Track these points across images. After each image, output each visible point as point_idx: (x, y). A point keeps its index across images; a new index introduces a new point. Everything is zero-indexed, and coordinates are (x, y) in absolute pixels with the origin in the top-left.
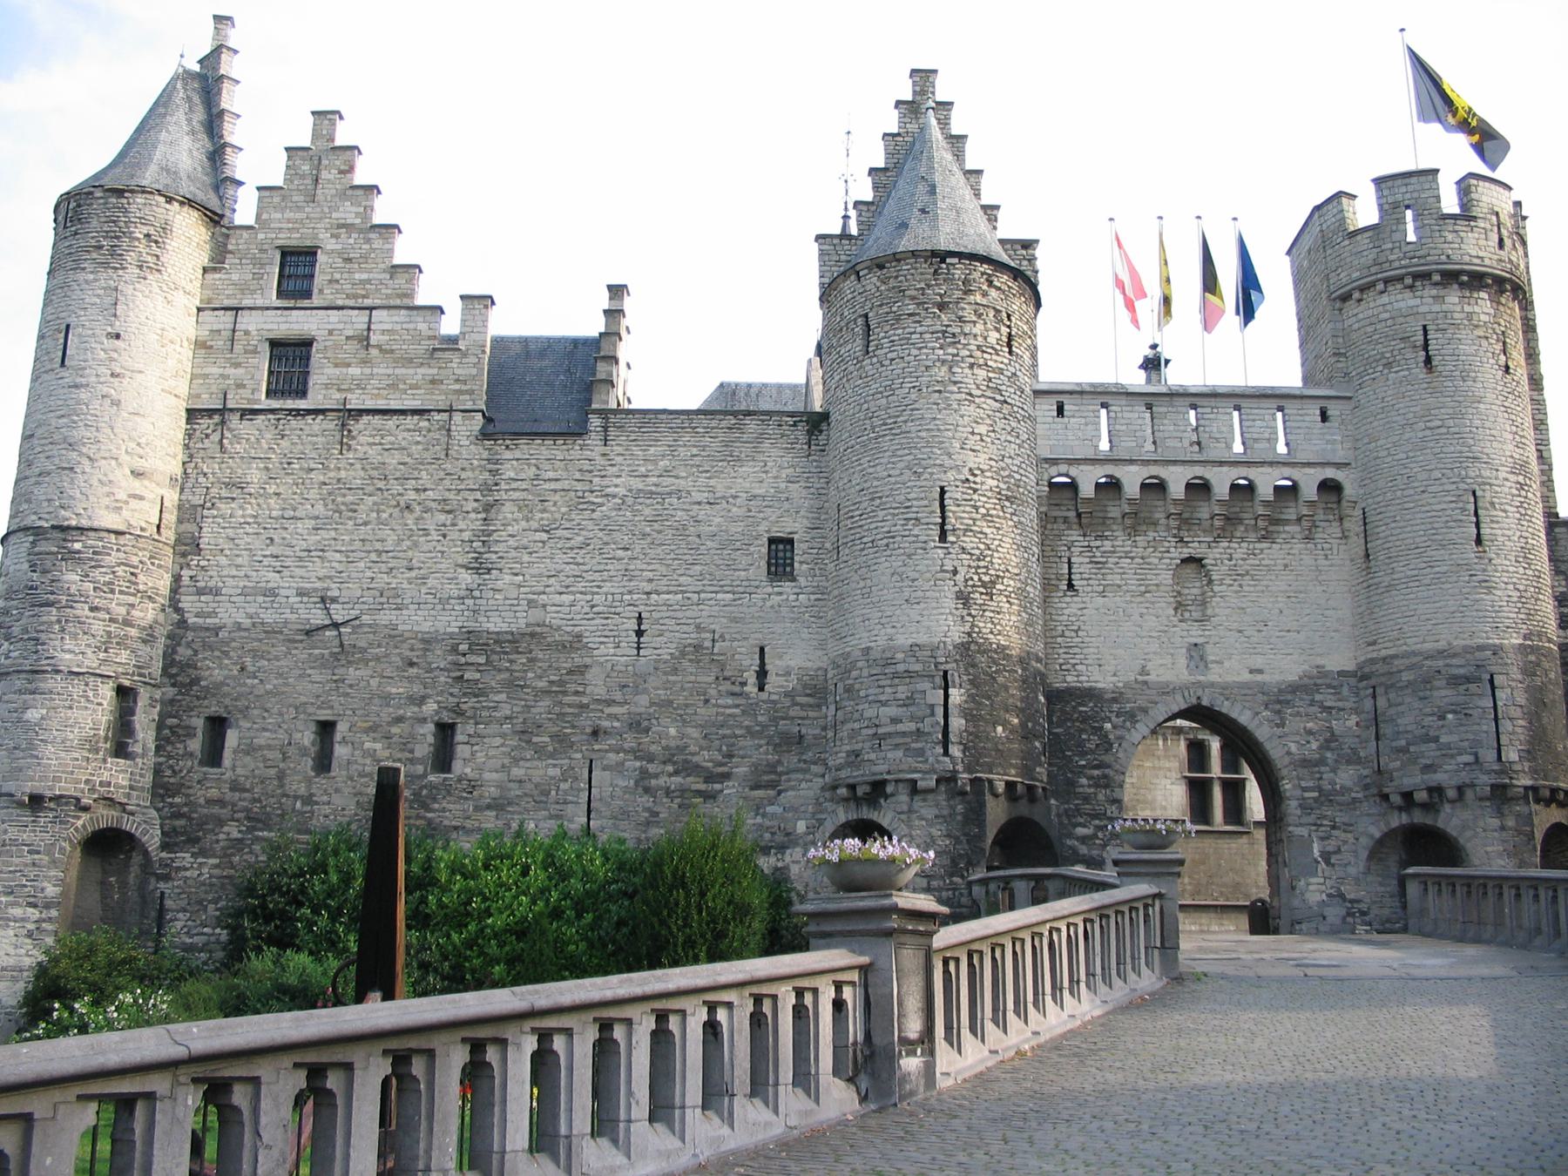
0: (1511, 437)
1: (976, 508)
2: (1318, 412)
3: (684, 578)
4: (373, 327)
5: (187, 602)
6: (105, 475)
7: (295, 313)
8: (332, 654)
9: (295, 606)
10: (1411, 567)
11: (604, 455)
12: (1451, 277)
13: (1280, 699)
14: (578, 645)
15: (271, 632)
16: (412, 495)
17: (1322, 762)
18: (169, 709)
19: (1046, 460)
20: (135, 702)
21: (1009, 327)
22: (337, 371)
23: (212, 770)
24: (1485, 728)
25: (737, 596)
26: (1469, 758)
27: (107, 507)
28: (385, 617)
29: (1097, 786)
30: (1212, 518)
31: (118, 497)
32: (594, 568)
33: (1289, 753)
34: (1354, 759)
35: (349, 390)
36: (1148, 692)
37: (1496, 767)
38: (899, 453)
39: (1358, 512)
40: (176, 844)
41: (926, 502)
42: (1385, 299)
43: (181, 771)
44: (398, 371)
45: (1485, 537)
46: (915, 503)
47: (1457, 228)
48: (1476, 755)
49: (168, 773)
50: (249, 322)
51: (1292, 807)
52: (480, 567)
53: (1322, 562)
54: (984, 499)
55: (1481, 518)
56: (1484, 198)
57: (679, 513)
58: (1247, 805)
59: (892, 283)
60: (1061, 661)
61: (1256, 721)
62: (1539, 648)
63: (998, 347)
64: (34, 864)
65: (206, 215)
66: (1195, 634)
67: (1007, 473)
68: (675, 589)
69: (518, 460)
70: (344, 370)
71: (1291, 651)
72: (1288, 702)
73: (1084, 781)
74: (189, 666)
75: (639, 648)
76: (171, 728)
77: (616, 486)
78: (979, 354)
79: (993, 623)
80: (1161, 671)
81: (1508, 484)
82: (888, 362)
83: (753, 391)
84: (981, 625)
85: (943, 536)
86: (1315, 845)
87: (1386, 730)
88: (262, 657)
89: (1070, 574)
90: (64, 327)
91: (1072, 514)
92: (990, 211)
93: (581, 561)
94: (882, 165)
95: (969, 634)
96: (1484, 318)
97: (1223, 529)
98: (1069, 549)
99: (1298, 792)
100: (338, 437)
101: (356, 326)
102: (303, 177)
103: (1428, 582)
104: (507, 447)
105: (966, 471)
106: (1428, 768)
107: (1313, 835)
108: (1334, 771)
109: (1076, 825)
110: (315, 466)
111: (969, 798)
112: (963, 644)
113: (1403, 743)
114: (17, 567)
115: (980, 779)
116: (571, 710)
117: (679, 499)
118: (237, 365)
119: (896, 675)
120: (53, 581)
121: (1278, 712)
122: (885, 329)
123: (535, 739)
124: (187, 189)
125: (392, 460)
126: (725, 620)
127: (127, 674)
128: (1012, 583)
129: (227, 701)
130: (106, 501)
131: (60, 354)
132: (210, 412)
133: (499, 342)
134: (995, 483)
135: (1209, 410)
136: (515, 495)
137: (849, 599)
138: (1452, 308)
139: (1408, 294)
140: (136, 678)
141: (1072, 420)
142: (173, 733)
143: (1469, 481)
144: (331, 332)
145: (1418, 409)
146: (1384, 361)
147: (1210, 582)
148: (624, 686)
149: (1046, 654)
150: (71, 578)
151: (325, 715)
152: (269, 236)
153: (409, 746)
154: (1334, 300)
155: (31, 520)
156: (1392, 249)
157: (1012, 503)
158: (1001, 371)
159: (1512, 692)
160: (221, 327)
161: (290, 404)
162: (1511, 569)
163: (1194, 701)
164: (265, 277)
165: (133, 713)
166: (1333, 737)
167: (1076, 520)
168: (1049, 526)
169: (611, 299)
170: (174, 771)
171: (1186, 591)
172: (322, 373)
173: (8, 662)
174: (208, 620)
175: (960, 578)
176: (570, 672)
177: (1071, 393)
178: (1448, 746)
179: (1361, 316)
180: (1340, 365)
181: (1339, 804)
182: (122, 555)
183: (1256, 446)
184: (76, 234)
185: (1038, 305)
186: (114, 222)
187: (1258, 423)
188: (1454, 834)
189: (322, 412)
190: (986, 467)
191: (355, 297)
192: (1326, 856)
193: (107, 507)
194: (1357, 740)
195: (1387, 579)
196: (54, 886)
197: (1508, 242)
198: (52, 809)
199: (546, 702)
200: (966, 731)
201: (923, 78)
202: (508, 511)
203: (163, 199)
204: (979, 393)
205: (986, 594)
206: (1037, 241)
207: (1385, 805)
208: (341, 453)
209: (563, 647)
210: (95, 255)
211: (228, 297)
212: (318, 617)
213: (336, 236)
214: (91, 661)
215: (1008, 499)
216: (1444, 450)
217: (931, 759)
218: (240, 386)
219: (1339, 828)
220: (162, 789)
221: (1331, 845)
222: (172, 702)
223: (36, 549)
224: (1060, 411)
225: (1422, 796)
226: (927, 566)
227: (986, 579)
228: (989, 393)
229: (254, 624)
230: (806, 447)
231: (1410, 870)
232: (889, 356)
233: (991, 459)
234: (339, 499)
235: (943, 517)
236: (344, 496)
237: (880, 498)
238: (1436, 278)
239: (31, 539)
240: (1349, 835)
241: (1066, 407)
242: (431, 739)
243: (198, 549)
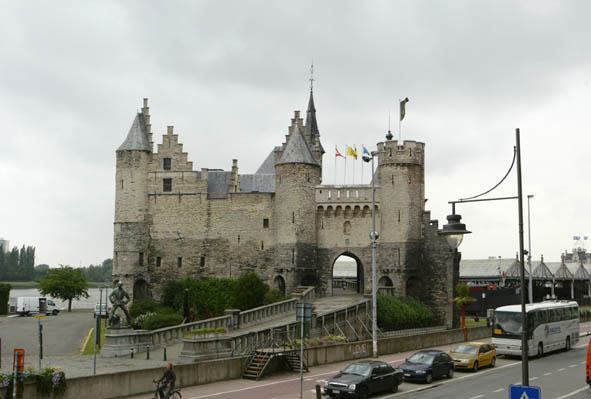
5: (152, 234)
12: (398, 164)
13: (364, 250)
15: (168, 240)
50: (159, 175)
52: (208, 226)
66: (347, 237)
112: (297, 244)
159: (403, 253)
202: (213, 215)
212: (177, 237)
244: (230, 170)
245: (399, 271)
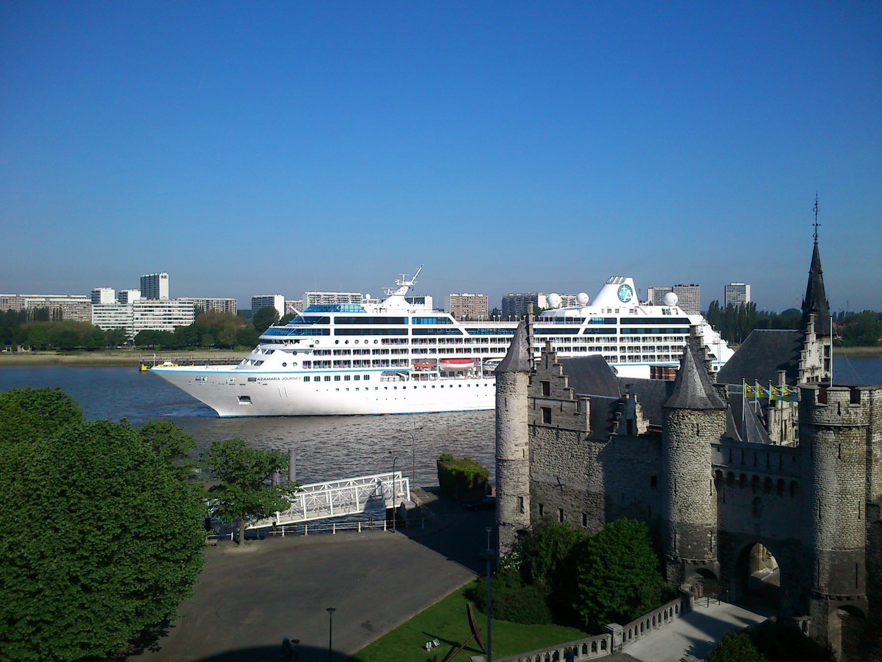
5: (533, 474)
28: (571, 484)
96: (830, 440)
130: (510, 453)
144: (554, 406)
158: (693, 443)
197: (843, 412)
214: (511, 492)
215: (695, 481)
227: (686, 505)
228: (689, 450)
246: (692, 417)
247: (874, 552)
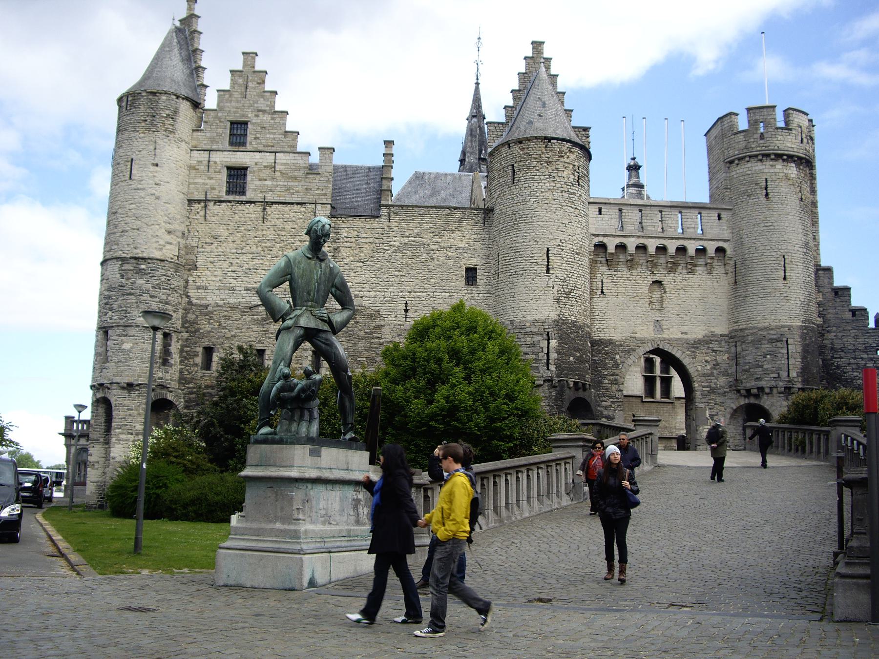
0: (802, 231)
1: (562, 258)
2: (717, 215)
3: (427, 285)
4: (277, 161)
5: (192, 293)
6: (154, 233)
7: (238, 153)
8: (262, 318)
9: (244, 295)
10: (755, 289)
11: (388, 226)
12: (779, 156)
13: (695, 346)
14: (378, 316)
15: (233, 308)
16: (298, 243)
17: (712, 374)
18: (187, 343)
19: (594, 235)
20: (171, 340)
21: (578, 173)
22: (260, 183)
23: (206, 372)
24: (783, 362)
25: (451, 294)
26: (775, 375)
27: (156, 248)
29: (612, 384)
30: (667, 263)
31: (162, 243)
32: (385, 280)
33: (697, 371)
34: (725, 374)
35: (266, 192)
36: (636, 342)
37: (787, 380)
38: (528, 231)
39: (732, 263)
40: (191, 406)
41: (541, 255)
42: (749, 165)
43: (192, 372)
44: (289, 184)
45: (787, 277)
46: (535, 255)
47: (783, 134)
48: (779, 374)
49: (186, 373)
50: (217, 157)
51: (698, 394)
53: (715, 284)
54: (567, 254)
55: (787, 268)
56: (795, 120)
57: (424, 255)
58: (672, 389)
59: (526, 151)
60: (598, 327)
61: (683, 356)
62: (808, 327)
63: (574, 183)
64: (130, 415)
65: (193, 104)
66: (657, 316)
67: (576, 242)
68: (422, 290)
69: (348, 228)
70: (264, 182)
71: (700, 324)
72: (697, 348)
73: (606, 381)
74: (194, 323)
75: (406, 318)
76: (186, 352)
77: (395, 241)
78: (565, 186)
79: (569, 310)
80: (642, 332)
81: (799, 253)
82: (524, 189)
83: (432, 176)
84: (564, 311)
85: (548, 271)
86: (707, 411)
87: (741, 361)
88: (229, 319)
89: (602, 287)
90: (130, 159)
91: (603, 260)
92: (569, 112)
93: (379, 276)
94: (517, 88)
95: (559, 316)
96: (793, 176)
97: (671, 268)
98: (602, 275)
99: (701, 388)
100: (262, 214)
101: (268, 161)
102: (239, 85)
103: (762, 296)
104: (343, 221)
105: (559, 240)
106: (758, 379)
107: (707, 407)
108: (717, 379)
109: (602, 401)
110: (251, 229)
111: (558, 389)
113: (747, 367)
114: (113, 276)
115: (563, 380)
116: (375, 346)
117: (424, 248)
118: (211, 178)
119: (526, 333)
120: (132, 283)
121: (694, 352)
122: (522, 173)
123: (359, 359)
124: (184, 92)
125: (288, 227)
126: (445, 305)
127: (168, 327)
128: (578, 292)
129: (213, 340)
130: (155, 245)
131: (129, 173)
132: (199, 201)
133: (336, 168)
134: (571, 246)
135: (667, 213)
136: (348, 244)
137: (504, 298)
138: (778, 171)
139: (759, 164)
140: (171, 329)
141: (606, 216)
142: (188, 355)
143: (782, 251)
144: (256, 164)
145: (761, 217)
146: (748, 194)
147: (665, 292)
148: (400, 335)
149: (591, 324)
150: (140, 282)
151: (259, 347)
152: (224, 114)
153: (300, 361)
154: (726, 162)
155: (119, 254)
156: (753, 142)
157: (578, 255)
158: (574, 194)
159: (795, 348)
160: (202, 159)
161: (238, 198)
162: (798, 291)
163: (656, 347)
164: (223, 135)
165: (170, 346)
166: (717, 364)
167: (606, 262)
168: (593, 265)
169: (386, 147)
170: (189, 372)
171: (654, 296)
172: (252, 182)
173: (111, 321)
174: (202, 302)
175: (556, 288)
176: (375, 328)
177: (605, 203)
178: (767, 369)
179: (738, 171)
180: (727, 193)
181: (719, 394)
182: (163, 271)
183: (688, 230)
184: (133, 113)
185: (589, 157)
186: (152, 108)
187: (690, 220)
188: (767, 408)
189: (254, 202)
190: (567, 239)
191: (268, 146)
192: (712, 416)
193: (156, 248)
194: (727, 365)
195: (744, 294)
196: (140, 425)
197: (805, 140)
198: (137, 390)
199: (364, 342)
200: (557, 359)
201: (537, 45)
203: (174, 97)
204: (565, 204)
205: (567, 297)
206: (590, 128)
207: (738, 395)
208: (264, 223)
209: (371, 317)
210: (143, 124)
211: (205, 144)
213: (257, 116)
215: (577, 254)
216: (772, 236)
217: (541, 371)
218: (214, 189)
219: (718, 404)
220: (183, 380)
221: (714, 412)
222: (187, 340)
223: (123, 268)
224: (600, 212)
225: (755, 391)
226: (541, 284)
227: (567, 290)
229: (224, 304)
230: (482, 225)
231: (748, 424)
232: (524, 185)
233: (569, 235)
234: (264, 245)
235: (548, 262)
236: (266, 243)
237: (519, 252)
238: (773, 157)
239: (120, 263)
240: (722, 408)
241: (603, 210)
242: (310, 358)
243: (196, 268)
244: (380, 162)
245: (788, 391)
246: (572, 156)
247: (828, 331)
